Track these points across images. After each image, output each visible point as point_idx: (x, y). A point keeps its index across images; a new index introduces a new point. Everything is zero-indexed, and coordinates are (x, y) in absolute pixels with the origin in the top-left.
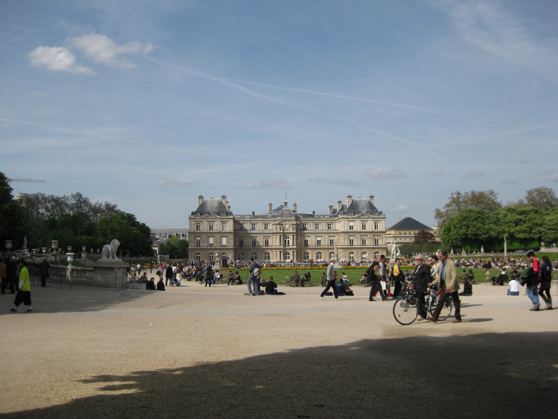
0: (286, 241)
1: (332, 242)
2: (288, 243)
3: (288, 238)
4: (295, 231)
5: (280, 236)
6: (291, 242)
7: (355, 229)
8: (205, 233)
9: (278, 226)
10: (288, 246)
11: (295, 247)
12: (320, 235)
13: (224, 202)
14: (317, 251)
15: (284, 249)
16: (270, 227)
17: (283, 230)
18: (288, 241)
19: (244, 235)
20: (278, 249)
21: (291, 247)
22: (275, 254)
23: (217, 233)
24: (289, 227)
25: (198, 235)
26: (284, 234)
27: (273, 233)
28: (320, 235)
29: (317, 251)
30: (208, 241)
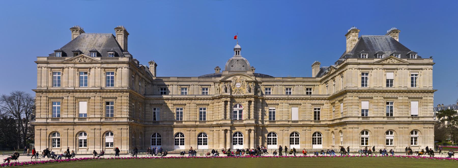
0: (236, 112)
1: (317, 115)
2: (241, 116)
3: (240, 106)
4: (252, 93)
5: (226, 102)
6: (245, 113)
7: (371, 84)
8: (69, 92)
9: (222, 84)
10: (241, 120)
11: (253, 122)
12: (297, 102)
13: (120, 39)
14: (291, 130)
15: (233, 127)
16: (212, 91)
17: (231, 91)
18: (241, 112)
19: (161, 102)
20: (221, 126)
21: (245, 122)
22: (215, 134)
23: (95, 92)
24: (241, 86)
25: (54, 95)
26: (232, 98)
27: (213, 99)
28: (297, 102)
29: (291, 130)
30: (76, 107)
